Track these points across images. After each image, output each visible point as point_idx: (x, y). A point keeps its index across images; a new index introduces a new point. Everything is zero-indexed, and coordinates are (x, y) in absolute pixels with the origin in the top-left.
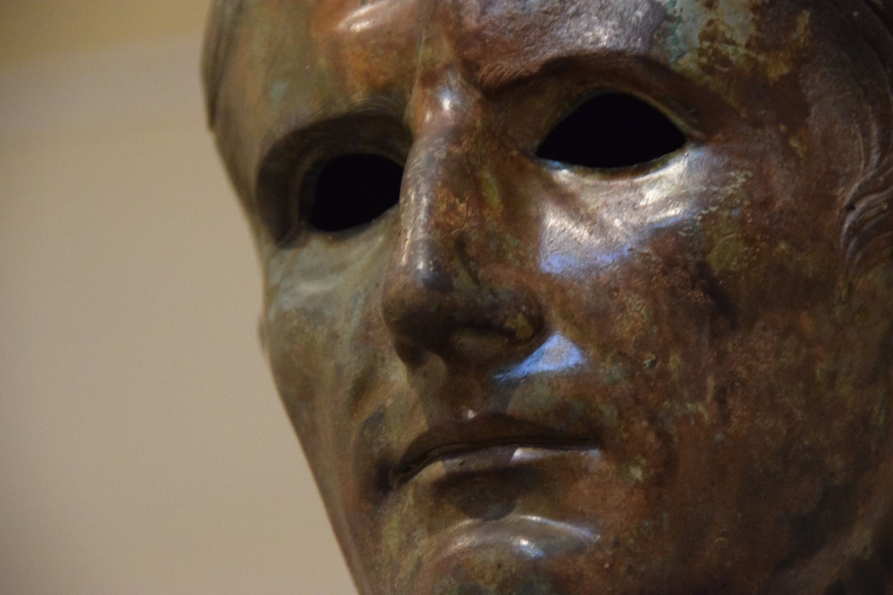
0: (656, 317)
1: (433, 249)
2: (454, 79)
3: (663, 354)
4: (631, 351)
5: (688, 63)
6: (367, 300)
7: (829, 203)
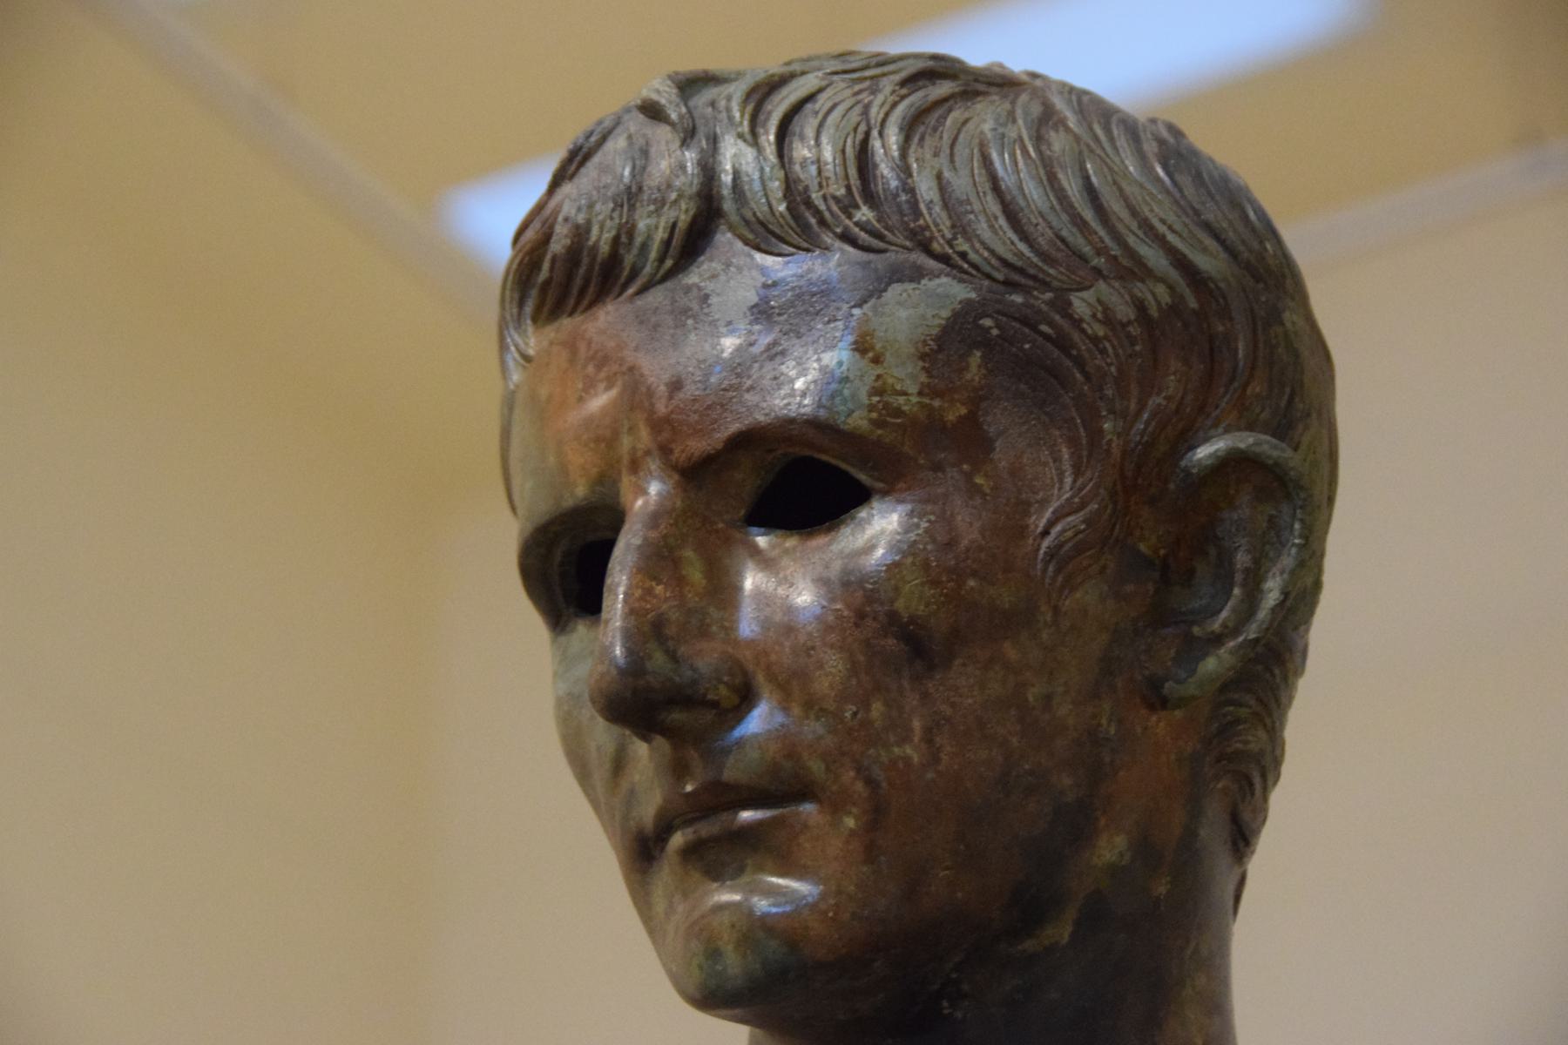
0: (854, 669)
1: (628, 636)
2: (654, 465)
3: (866, 706)
4: (831, 706)
7: (1021, 532)
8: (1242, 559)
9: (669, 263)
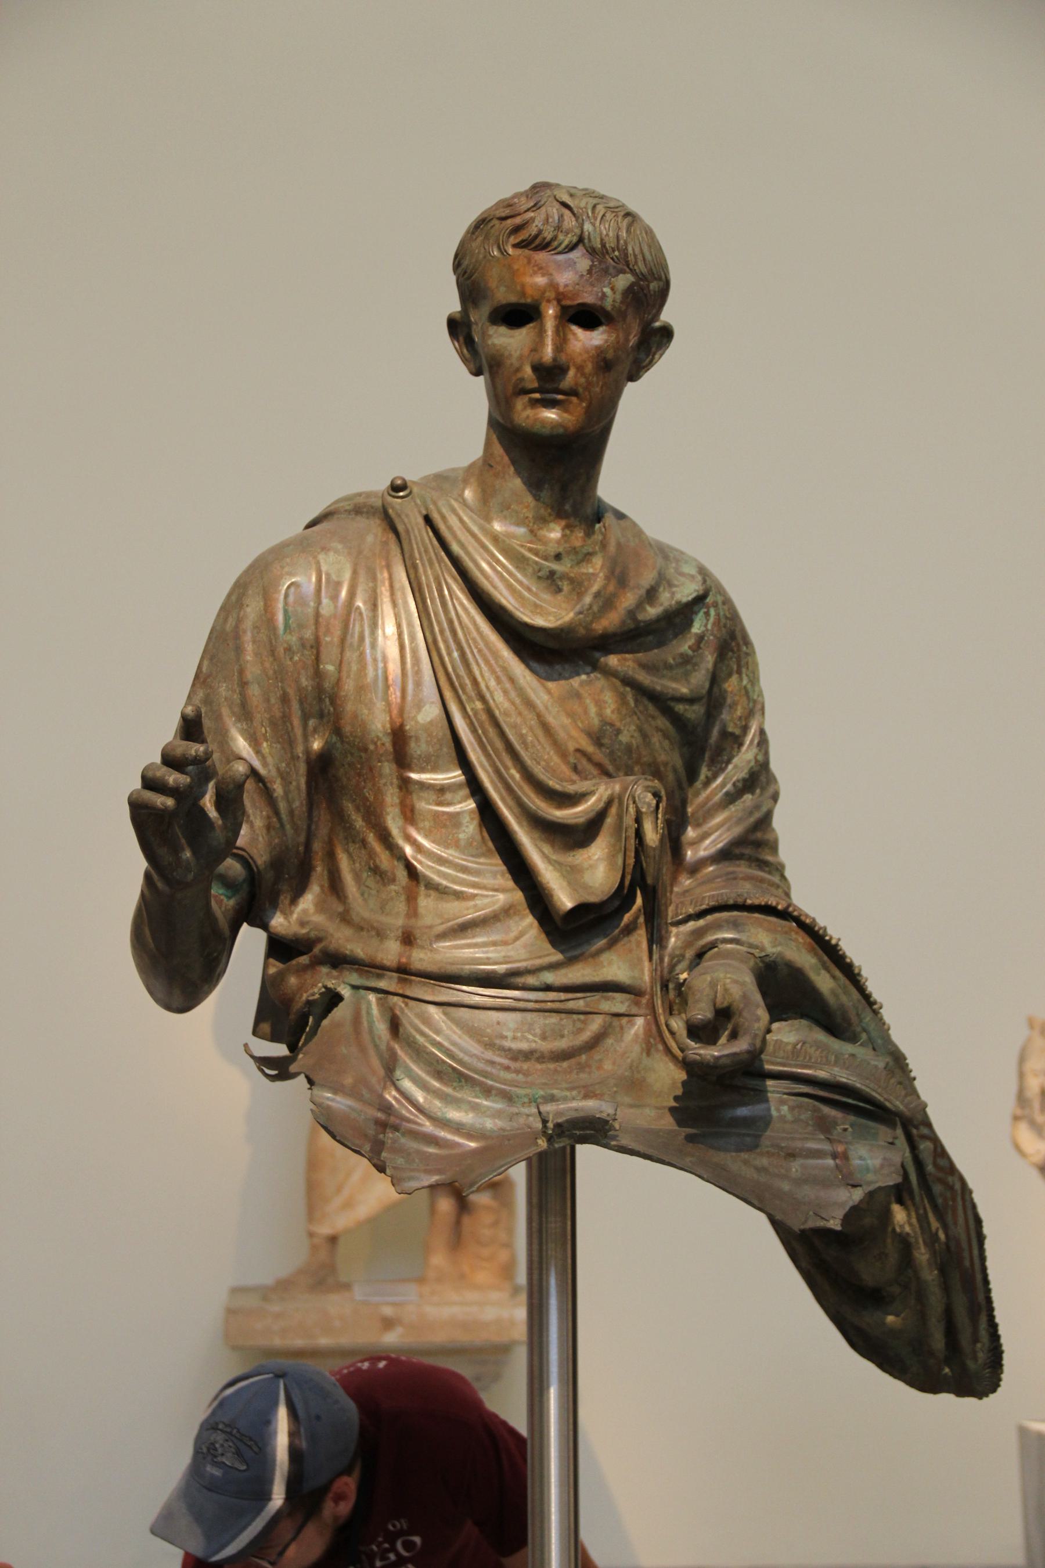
2: (555, 303)
5: (609, 308)
8: (653, 350)
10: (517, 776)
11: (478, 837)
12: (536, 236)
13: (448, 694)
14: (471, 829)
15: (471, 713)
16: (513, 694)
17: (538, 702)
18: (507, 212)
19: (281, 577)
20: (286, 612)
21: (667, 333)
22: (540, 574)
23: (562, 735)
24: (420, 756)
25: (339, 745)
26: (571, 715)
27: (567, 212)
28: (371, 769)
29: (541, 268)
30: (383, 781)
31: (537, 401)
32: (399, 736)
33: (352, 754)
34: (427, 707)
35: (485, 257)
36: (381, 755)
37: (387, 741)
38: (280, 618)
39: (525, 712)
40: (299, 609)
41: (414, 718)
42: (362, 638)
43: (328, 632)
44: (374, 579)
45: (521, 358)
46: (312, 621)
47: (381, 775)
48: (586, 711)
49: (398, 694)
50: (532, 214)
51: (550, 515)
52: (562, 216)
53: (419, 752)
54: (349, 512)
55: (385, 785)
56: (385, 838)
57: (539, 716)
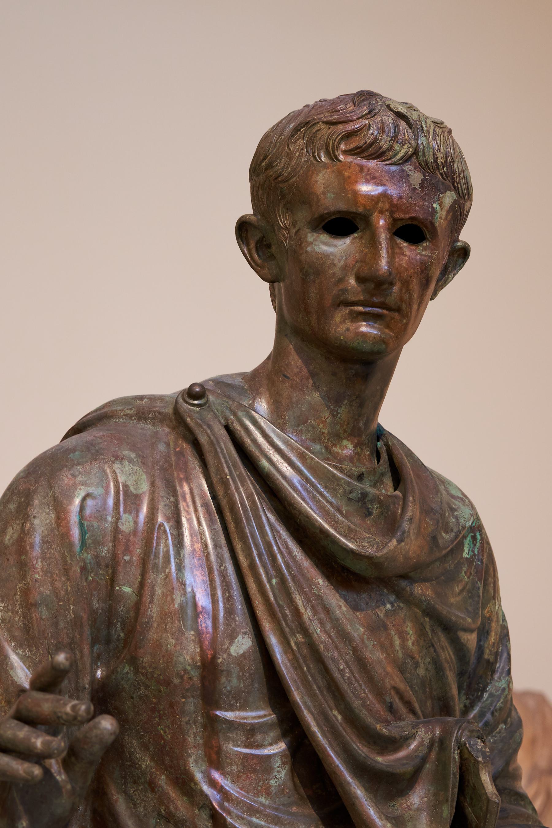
2: (387, 214)
6: (346, 259)
9: (401, 161)
10: (340, 717)
11: (290, 784)
12: (371, 145)
13: (267, 626)
14: (281, 774)
15: (295, 648)
16: (328, 626)
17: (355, 635)
18: (335, 117)
19: (75, 487)
20: (81, 525)
21: (464, 253)
22: (350, 496)
23: (379, 671)
24: (230, 692)
25: (131, 676)
26: (383, 647)
27: (402, 124)
28: (171, 705)
29: (374, 178)
30: (185, 719)
31: (360, 313)
32: (209, 668)
33: (147, 687)
34: (240, 637)
35: (307, 161)
36: (187, 690)
37: (195, 674)
38: (76, 532)
39: (341, 646)
40: (96, 524)
41: (227, 650)
42: (167, 560)
43: (127, 550)
44: (174, 493)
45: (345, 268)
46: (109, 537)
47: (183, 712)
48: (392, 644)
49: (209, 623)
50: (367, 122)
51: (345, 431)
52: (398, 126)
53: (229, 688)
54: (131, 417)
55: (187, 723)
56: (185, 784)
57: (355, 650)
